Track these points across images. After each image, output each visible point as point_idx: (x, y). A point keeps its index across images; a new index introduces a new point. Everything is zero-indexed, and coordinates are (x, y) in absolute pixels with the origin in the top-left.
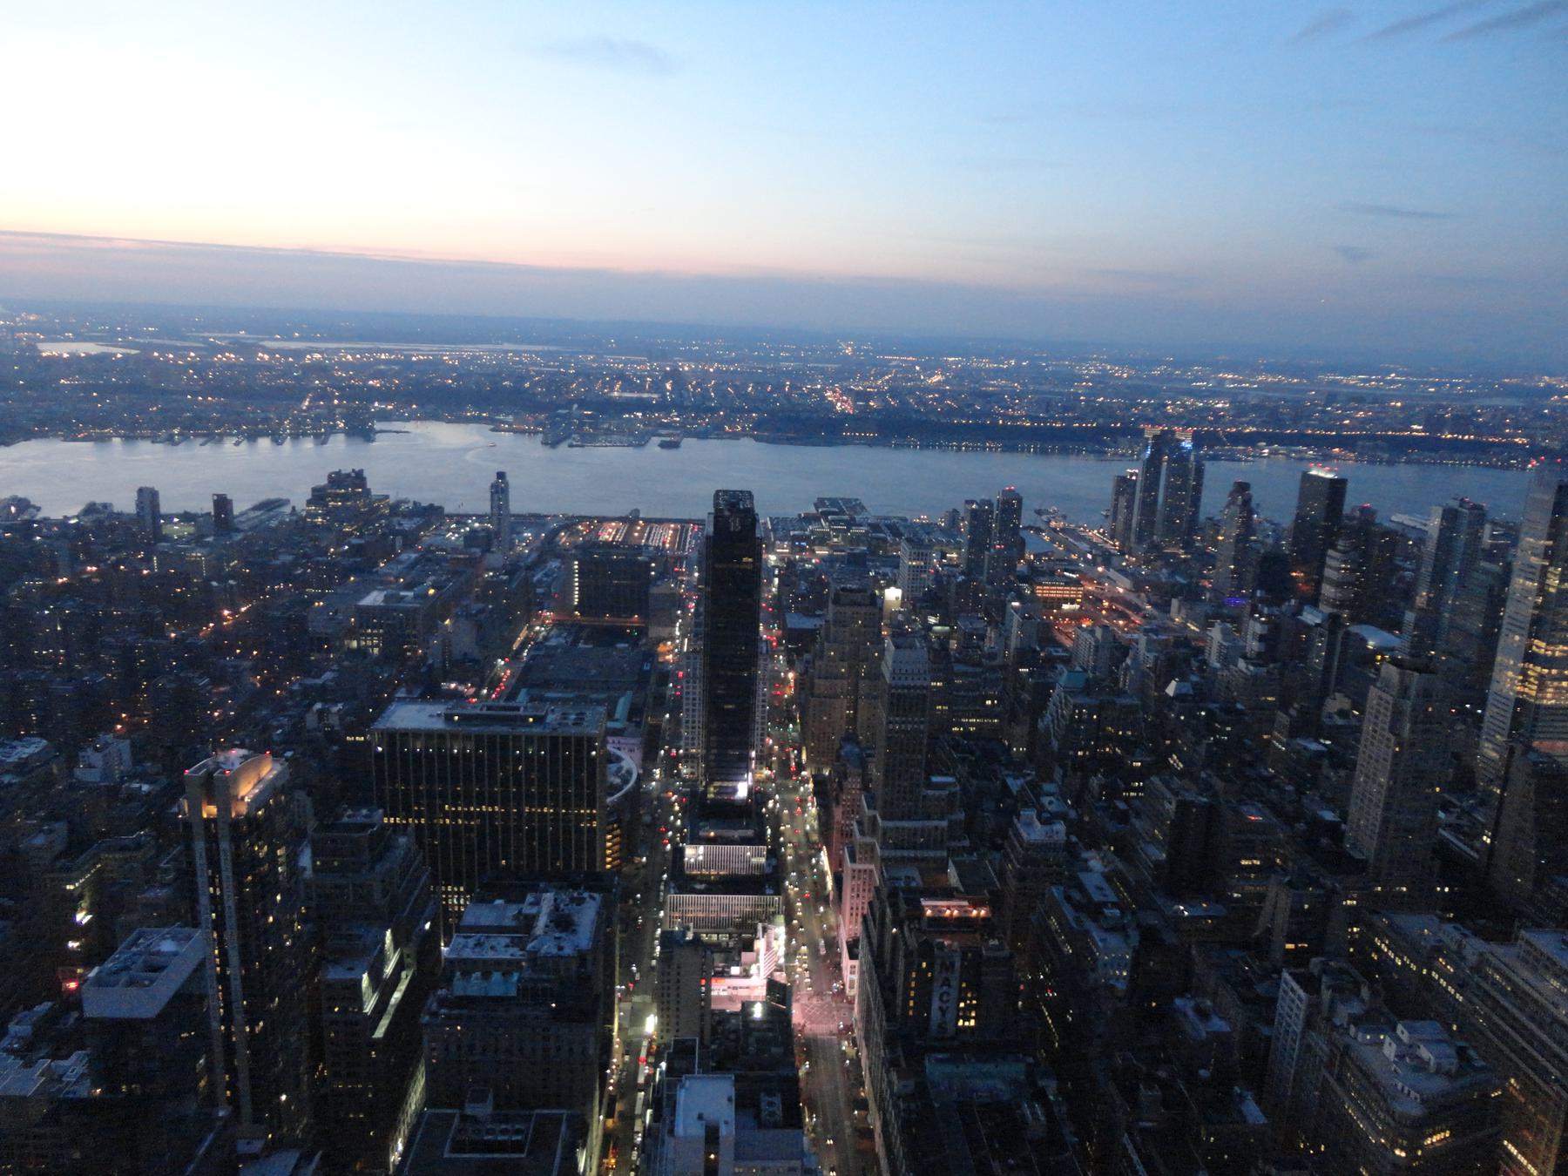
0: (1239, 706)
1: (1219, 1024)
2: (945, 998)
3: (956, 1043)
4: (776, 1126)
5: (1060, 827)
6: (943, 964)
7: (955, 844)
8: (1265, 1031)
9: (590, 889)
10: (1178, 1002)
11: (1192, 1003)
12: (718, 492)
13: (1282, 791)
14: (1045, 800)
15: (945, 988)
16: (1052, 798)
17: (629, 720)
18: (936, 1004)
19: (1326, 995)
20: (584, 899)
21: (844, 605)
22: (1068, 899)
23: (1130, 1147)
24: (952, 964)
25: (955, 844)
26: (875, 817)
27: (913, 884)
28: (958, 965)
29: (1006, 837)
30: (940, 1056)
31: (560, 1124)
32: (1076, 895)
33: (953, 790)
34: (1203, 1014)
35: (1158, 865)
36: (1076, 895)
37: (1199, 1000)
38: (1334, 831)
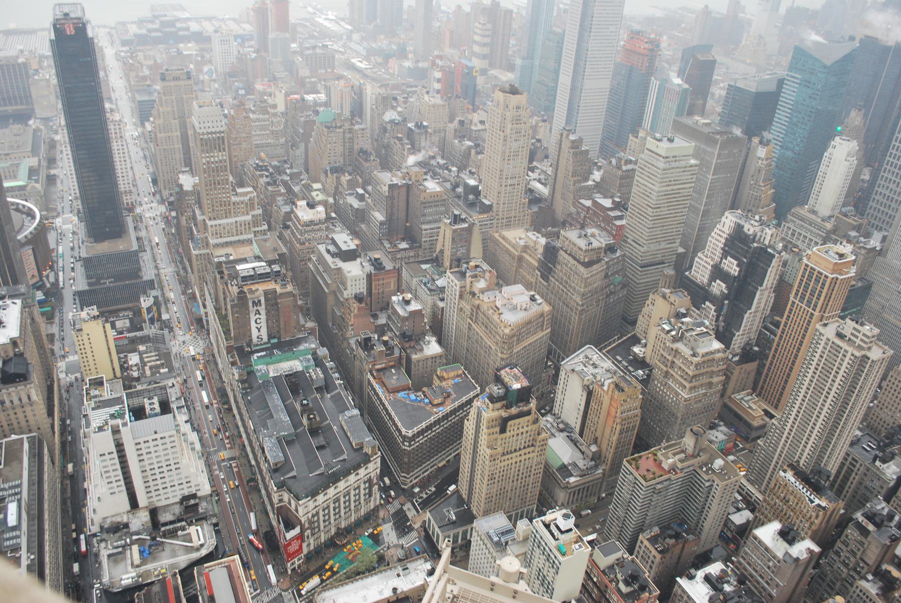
0: (425, 123)
1: (414, 306)
2: (258, 321)
3: (269, 345)
4: (156, 415)
5: (321, 209)
6: (254, 302)
7: (257, 229)
8: (441, 304)
9: (12, 297)
10: (394, 298)
11: (401, 298)
12: (55, 5)
13: (450, 171)
14: (314, 194)
15: (258, 316)
16: (318, 192)
17: (29, 178)
18: (253, 325)
19: (469, 280)
20: (7, 305)
21: (170, 81)
22: (328, 251)
23: (371, 379)
24: (259, 301)
25: (257, 229)
26: (204, 220)
27: (231, 258)
28: (263, 301)
29: (291, 220)
30: (259, 354)
31: (22, 444)
32: (332, 248)
33: (252, 195)
34: (407, 302)
35: (382, 223)
36: (332, 248)
37: (404, 295)
38: (475, 191)
